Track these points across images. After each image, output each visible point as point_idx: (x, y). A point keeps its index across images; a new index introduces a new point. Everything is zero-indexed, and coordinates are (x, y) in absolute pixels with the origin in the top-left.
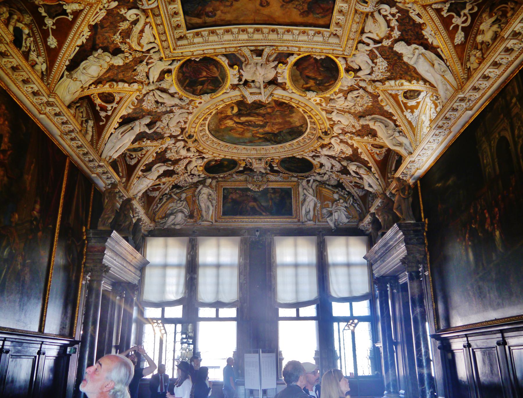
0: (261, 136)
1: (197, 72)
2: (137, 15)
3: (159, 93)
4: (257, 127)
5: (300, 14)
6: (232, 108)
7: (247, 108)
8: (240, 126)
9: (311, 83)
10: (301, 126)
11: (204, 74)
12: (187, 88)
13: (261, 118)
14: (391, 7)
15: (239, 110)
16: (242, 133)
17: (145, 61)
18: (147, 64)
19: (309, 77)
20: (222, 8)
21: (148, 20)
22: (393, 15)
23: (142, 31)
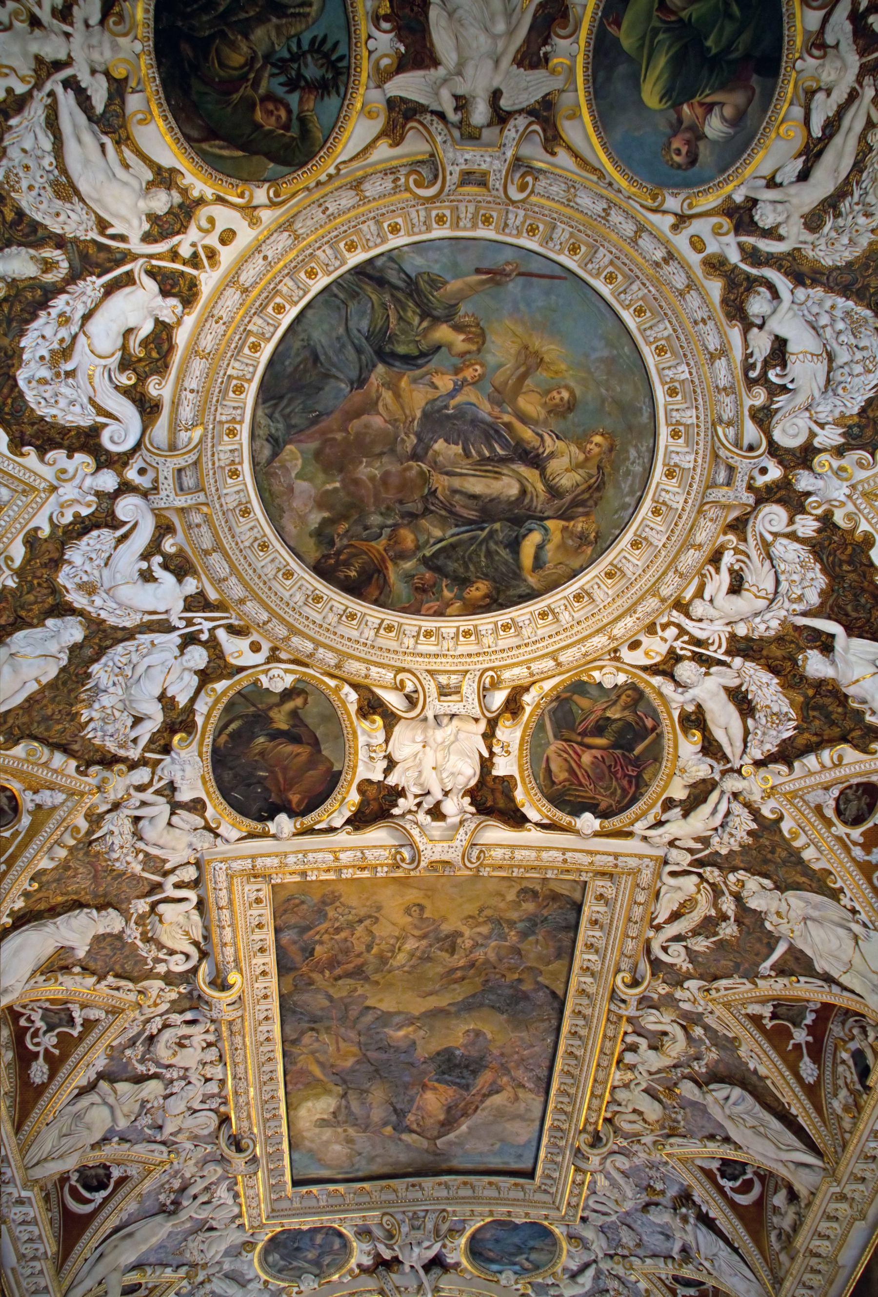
0: (443, 333)
1: (604, 771)
2: (665, 949)
3: (728, 750)
4: (461, 413)
5: (340, 896)
6: (538, 563)
7: (489, 554)
8: (527, 434)
9: (280, 720)
10: (276, 444)
11: (586, 758)
12: (649, 723)
13: (440, 482)
14: (169, 972)
15: (514, 546)
16: (531, 361)
17: (707, 852)
18: (705, 841)
19: (296, 739)
20: (502, 905)
21: (651, 934)
22: (157, 960)
23: (675, 916)
